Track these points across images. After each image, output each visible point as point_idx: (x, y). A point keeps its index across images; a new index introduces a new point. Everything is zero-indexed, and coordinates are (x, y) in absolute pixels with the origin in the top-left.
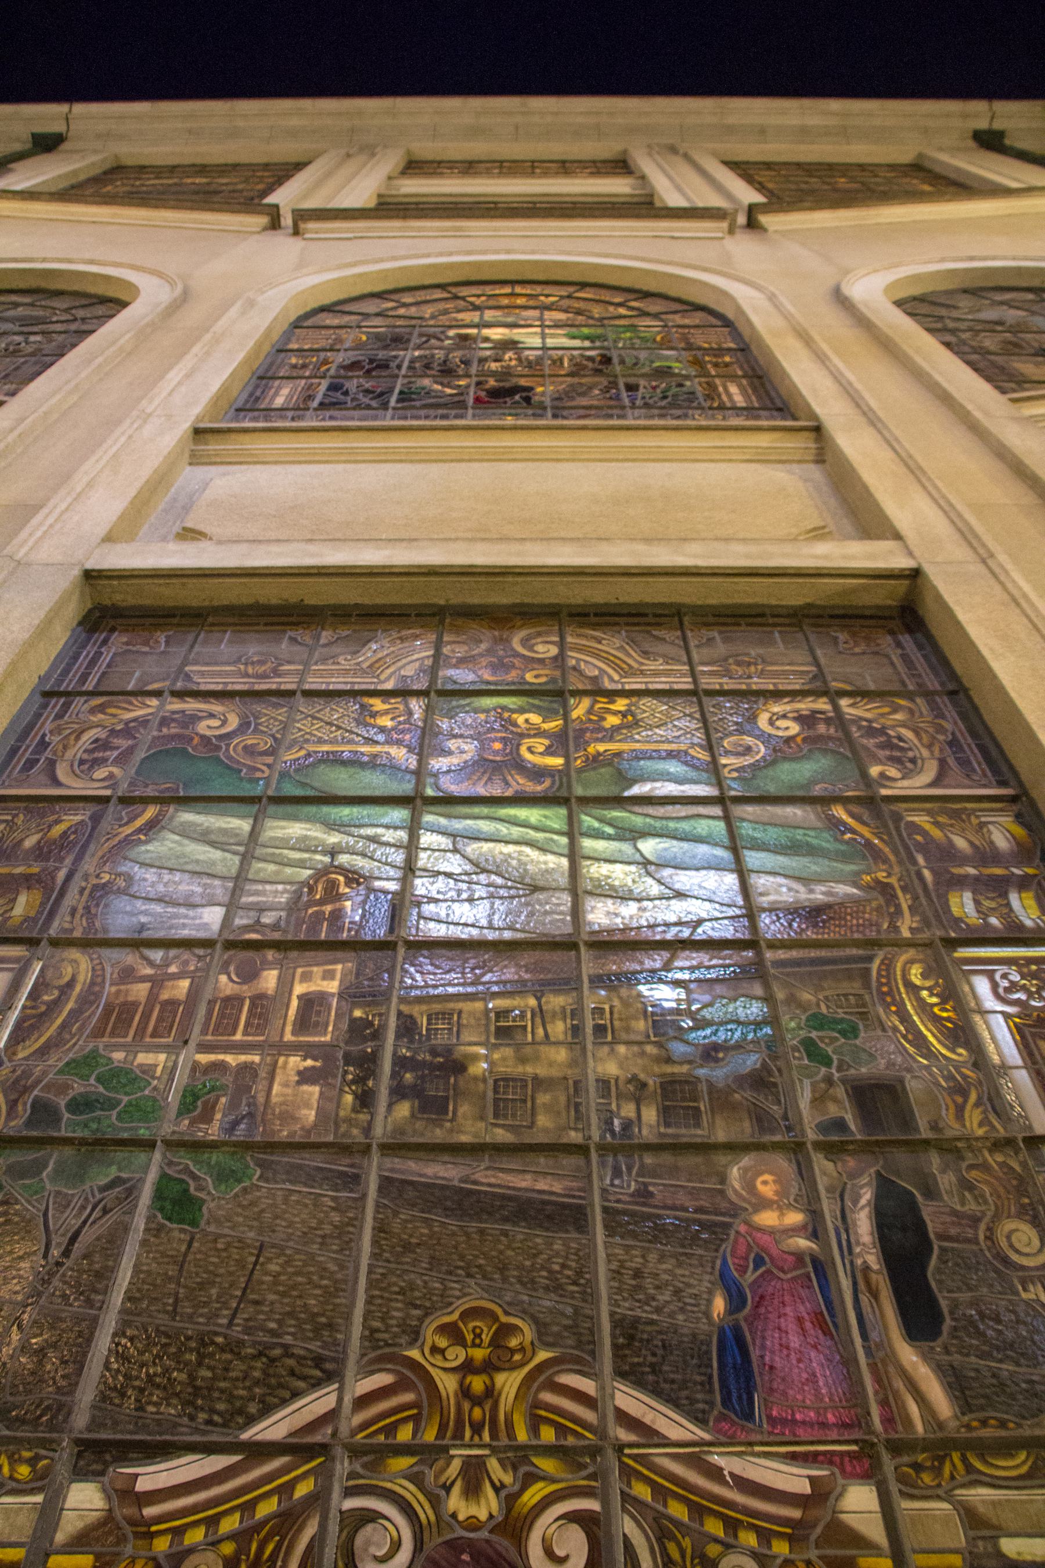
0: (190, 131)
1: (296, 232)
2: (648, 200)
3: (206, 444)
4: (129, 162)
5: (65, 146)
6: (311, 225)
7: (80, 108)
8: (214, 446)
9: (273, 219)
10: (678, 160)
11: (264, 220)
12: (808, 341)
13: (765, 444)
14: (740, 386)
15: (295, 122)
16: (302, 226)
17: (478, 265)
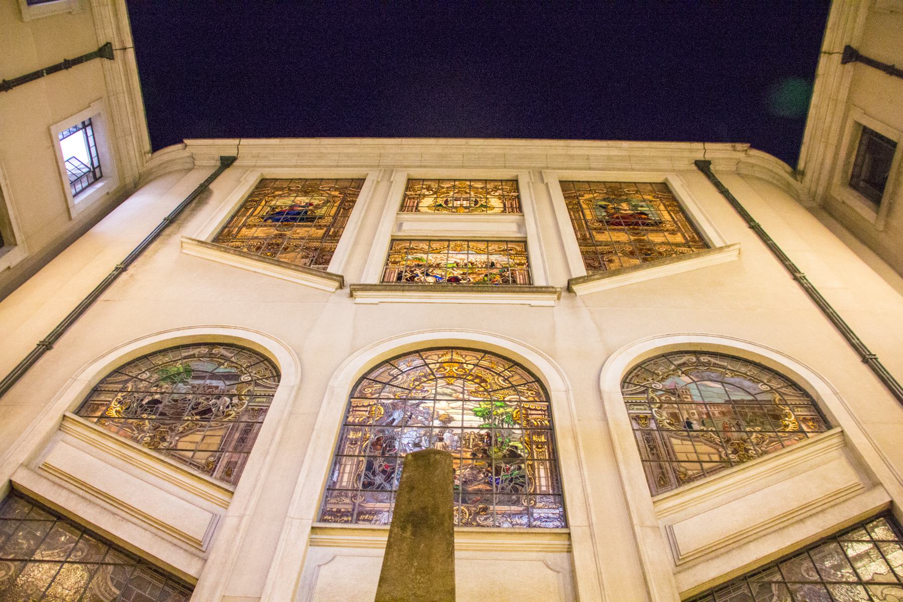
0: (298, 155)
1: (351, 295)
2: (524, 239)
3: (316, 534)
4: (268, 177)
5: (236, 163)
6: (359, 293)
7: (244, 141)
8: (320, 536)
9: (341, 284)
10: (542, 187)
11: (337, 284)
12: (575, 438)
13: (546, 542)
14: (545, 469)
15: (351, 150)
16: (354, 293)
17: (435, 341)
